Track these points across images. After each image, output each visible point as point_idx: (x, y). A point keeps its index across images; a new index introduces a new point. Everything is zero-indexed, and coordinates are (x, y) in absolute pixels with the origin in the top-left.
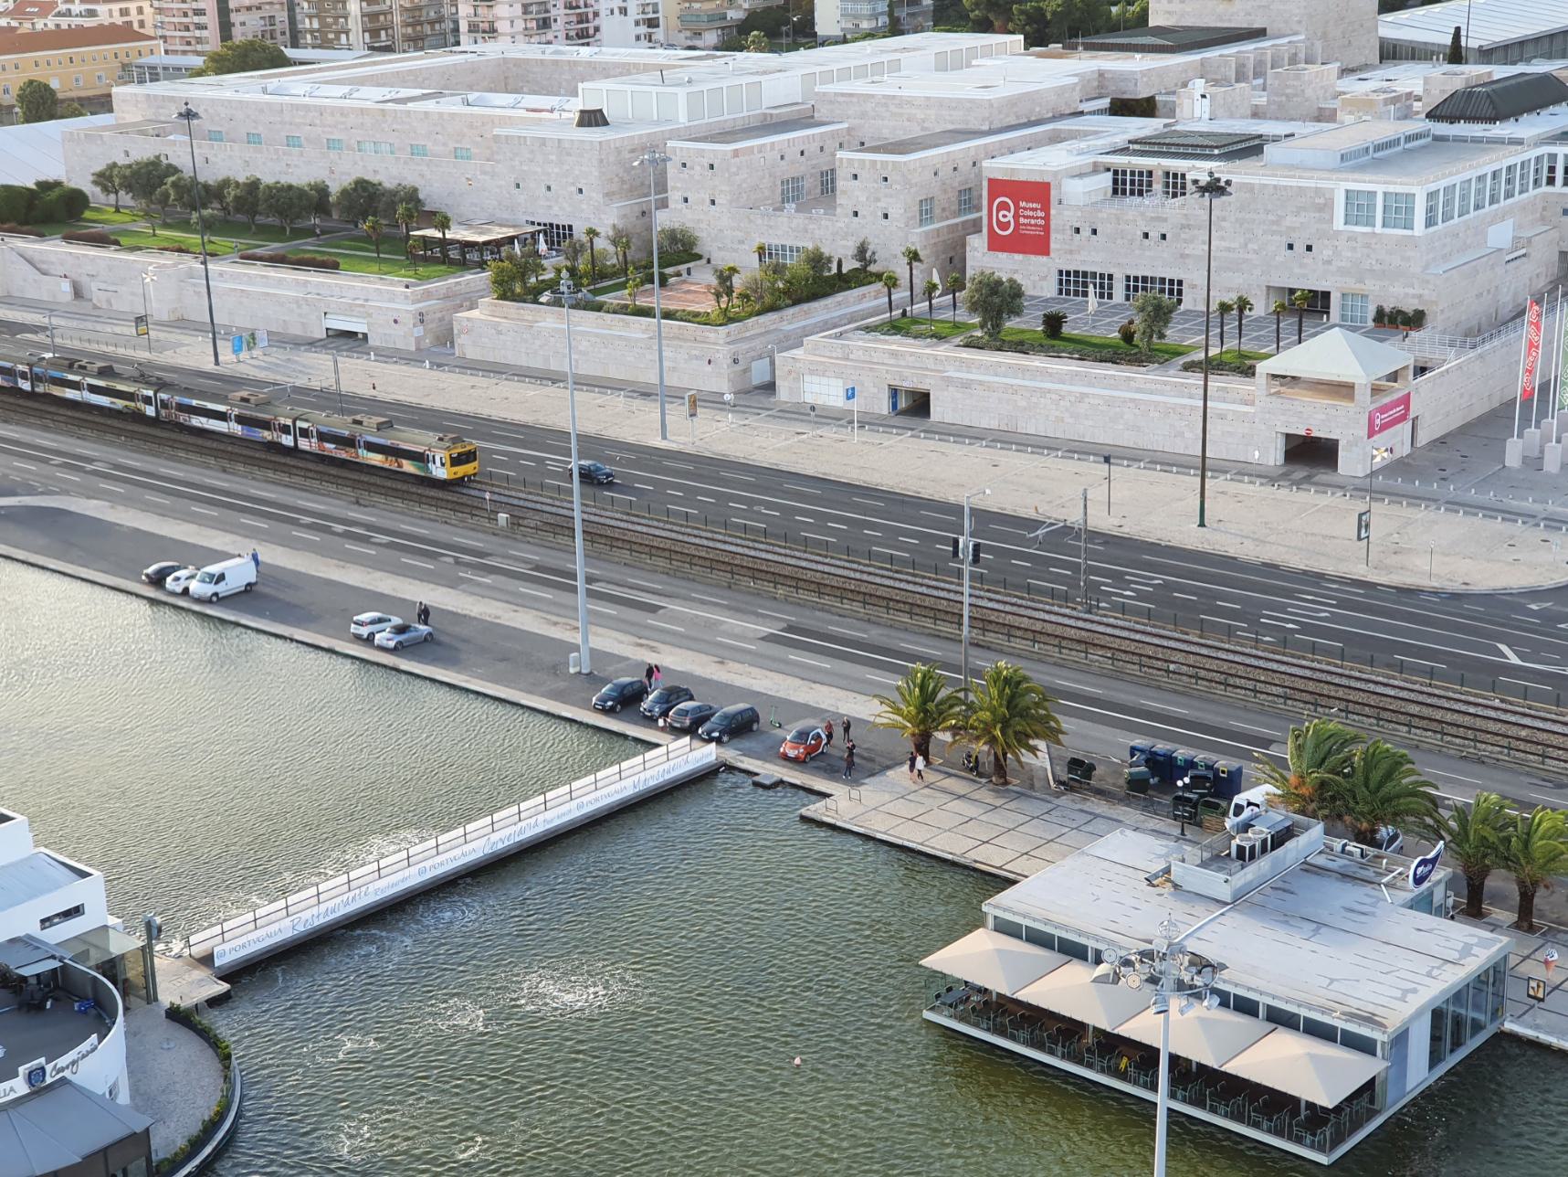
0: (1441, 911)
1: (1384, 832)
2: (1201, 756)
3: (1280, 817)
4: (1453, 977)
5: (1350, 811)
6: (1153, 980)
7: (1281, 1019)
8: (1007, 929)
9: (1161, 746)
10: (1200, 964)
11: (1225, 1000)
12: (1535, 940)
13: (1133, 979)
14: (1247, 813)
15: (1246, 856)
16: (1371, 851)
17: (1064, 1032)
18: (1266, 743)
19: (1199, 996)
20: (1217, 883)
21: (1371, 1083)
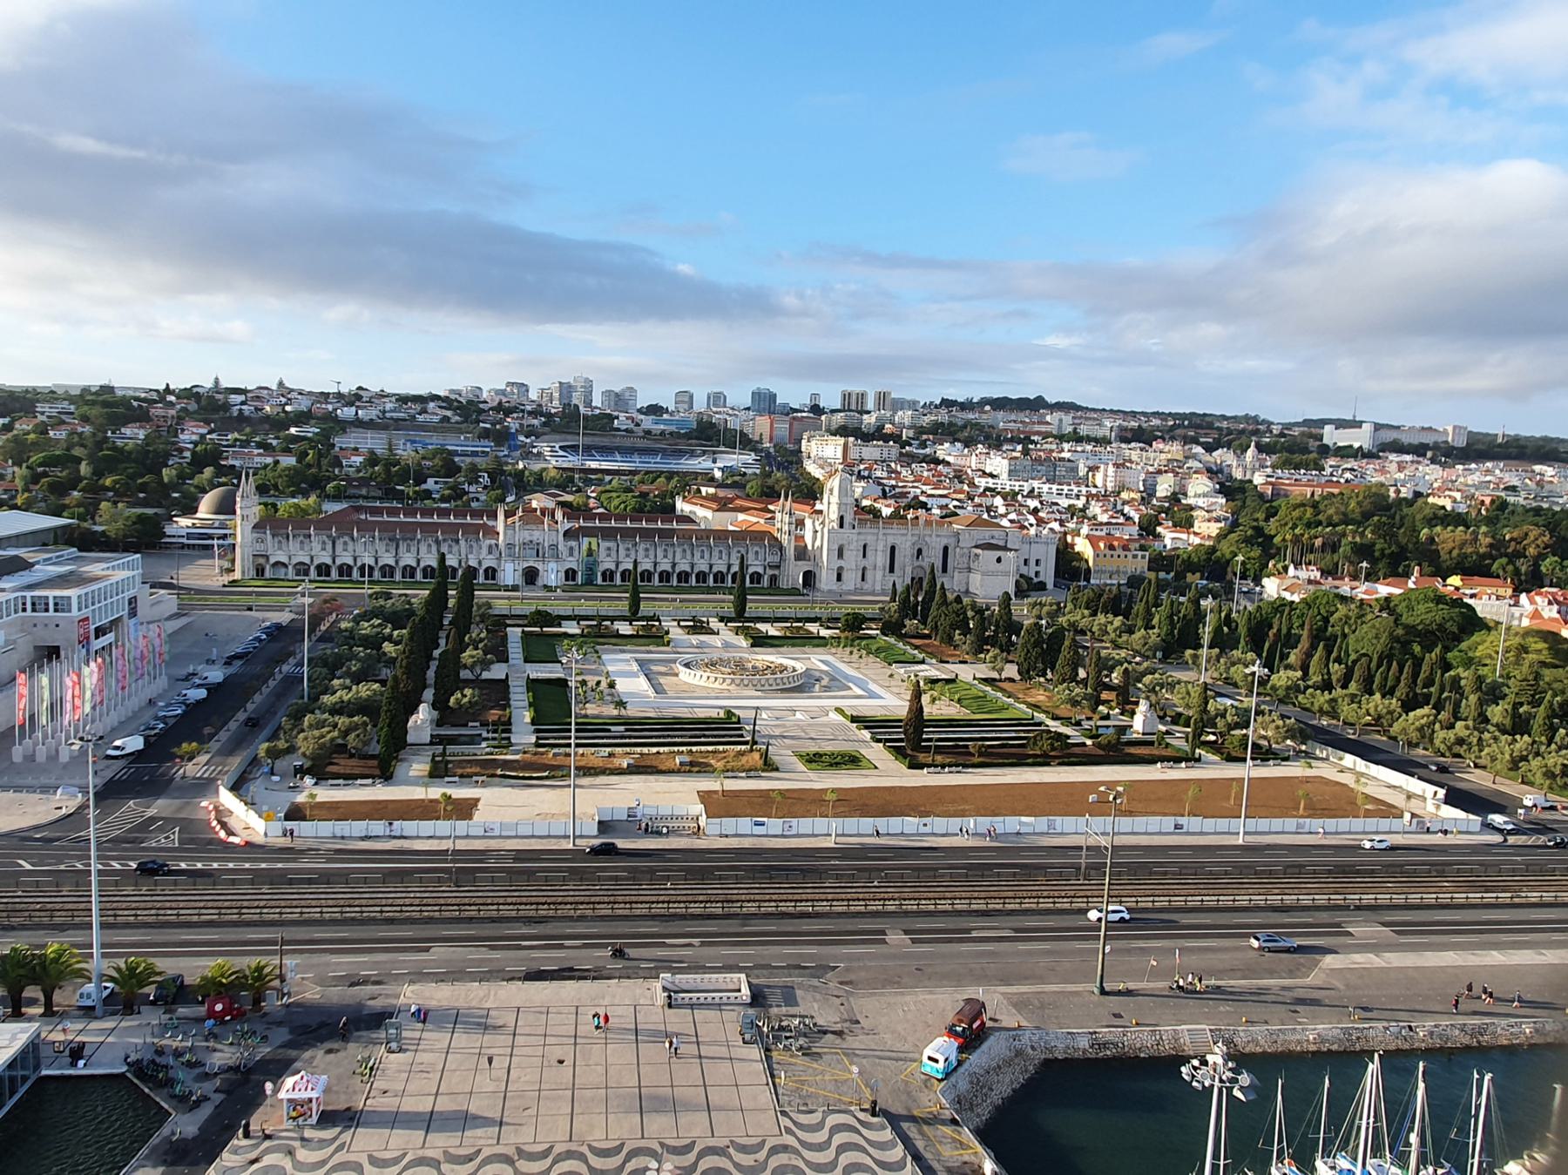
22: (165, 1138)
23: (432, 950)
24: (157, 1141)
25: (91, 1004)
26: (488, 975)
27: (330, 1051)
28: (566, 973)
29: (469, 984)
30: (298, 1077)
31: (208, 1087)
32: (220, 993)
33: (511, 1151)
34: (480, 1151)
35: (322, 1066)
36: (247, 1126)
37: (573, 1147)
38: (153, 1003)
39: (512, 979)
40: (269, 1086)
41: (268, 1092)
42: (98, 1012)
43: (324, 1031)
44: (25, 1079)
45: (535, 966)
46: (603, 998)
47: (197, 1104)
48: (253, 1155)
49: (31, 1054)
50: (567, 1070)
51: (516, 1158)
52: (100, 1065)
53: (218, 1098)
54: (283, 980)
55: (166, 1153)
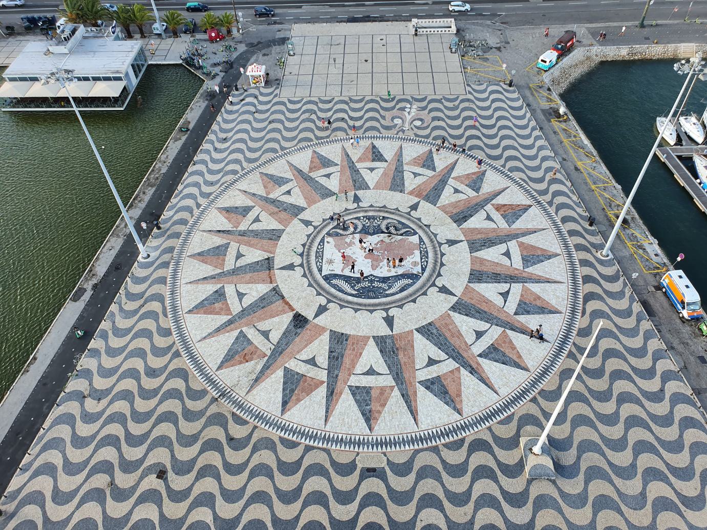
0: (123, 39)
1: (99, 22)
2: (41, 15)
3: (70, 26)
4: (132, 55)
5: (88, 19)
6: (58, 80)
7: (96, 79)
8: (12, 80)
9: (30, 15)
10: (68, 71)
11: (79, 79)
12: (147, 40)
13: (52, 81)
14: (62, 27)
15: (67, 39)
16: (98, 28)
17: (43, 101)
18: (57, 6)
19: (72, 80)
20: (62, 49)
21: (125, 87)
22: (205, 90)
23: (303, 7)
24: (202, 92)
25: (159, 32)
26: (330, 20)
27: (264, 55)
28: (367, 19)
29: (321, 25)
30: (253, 66)
31: (217, 70)
32: (213, 28)
33: (347, 99)
34: (334, 99)
35: (262, 61)
36: (236, 85)
37: (373, 98)
38: (185, 32)
39: (341, 22)
40: (242, 70)
41: (242, 72)
42: (164, 35)
43: (260, 46)
44: (143, 65)
45: (351, 15)
46: (385, 31)
47: (214, 77)
48: (242, 97)
49: (141, 53)
50: (369, 64)
51: (349, 102)
52: (170, 60)
53: (222, 74)
54: (238, 22)
55: (206, 96)
